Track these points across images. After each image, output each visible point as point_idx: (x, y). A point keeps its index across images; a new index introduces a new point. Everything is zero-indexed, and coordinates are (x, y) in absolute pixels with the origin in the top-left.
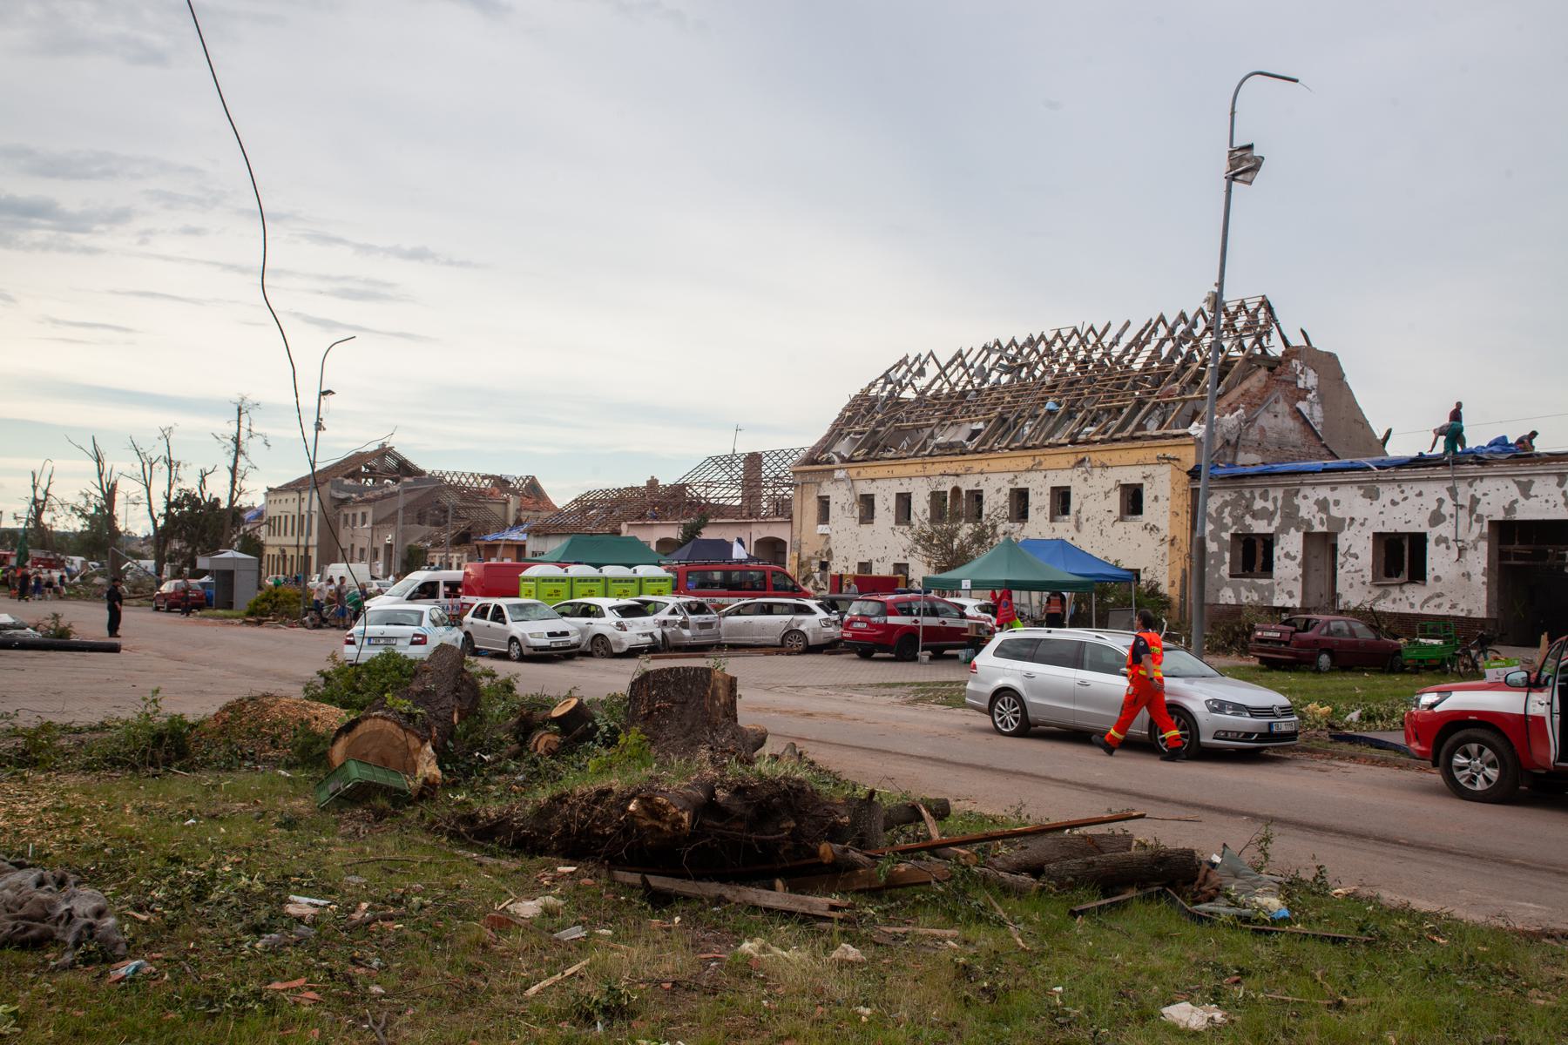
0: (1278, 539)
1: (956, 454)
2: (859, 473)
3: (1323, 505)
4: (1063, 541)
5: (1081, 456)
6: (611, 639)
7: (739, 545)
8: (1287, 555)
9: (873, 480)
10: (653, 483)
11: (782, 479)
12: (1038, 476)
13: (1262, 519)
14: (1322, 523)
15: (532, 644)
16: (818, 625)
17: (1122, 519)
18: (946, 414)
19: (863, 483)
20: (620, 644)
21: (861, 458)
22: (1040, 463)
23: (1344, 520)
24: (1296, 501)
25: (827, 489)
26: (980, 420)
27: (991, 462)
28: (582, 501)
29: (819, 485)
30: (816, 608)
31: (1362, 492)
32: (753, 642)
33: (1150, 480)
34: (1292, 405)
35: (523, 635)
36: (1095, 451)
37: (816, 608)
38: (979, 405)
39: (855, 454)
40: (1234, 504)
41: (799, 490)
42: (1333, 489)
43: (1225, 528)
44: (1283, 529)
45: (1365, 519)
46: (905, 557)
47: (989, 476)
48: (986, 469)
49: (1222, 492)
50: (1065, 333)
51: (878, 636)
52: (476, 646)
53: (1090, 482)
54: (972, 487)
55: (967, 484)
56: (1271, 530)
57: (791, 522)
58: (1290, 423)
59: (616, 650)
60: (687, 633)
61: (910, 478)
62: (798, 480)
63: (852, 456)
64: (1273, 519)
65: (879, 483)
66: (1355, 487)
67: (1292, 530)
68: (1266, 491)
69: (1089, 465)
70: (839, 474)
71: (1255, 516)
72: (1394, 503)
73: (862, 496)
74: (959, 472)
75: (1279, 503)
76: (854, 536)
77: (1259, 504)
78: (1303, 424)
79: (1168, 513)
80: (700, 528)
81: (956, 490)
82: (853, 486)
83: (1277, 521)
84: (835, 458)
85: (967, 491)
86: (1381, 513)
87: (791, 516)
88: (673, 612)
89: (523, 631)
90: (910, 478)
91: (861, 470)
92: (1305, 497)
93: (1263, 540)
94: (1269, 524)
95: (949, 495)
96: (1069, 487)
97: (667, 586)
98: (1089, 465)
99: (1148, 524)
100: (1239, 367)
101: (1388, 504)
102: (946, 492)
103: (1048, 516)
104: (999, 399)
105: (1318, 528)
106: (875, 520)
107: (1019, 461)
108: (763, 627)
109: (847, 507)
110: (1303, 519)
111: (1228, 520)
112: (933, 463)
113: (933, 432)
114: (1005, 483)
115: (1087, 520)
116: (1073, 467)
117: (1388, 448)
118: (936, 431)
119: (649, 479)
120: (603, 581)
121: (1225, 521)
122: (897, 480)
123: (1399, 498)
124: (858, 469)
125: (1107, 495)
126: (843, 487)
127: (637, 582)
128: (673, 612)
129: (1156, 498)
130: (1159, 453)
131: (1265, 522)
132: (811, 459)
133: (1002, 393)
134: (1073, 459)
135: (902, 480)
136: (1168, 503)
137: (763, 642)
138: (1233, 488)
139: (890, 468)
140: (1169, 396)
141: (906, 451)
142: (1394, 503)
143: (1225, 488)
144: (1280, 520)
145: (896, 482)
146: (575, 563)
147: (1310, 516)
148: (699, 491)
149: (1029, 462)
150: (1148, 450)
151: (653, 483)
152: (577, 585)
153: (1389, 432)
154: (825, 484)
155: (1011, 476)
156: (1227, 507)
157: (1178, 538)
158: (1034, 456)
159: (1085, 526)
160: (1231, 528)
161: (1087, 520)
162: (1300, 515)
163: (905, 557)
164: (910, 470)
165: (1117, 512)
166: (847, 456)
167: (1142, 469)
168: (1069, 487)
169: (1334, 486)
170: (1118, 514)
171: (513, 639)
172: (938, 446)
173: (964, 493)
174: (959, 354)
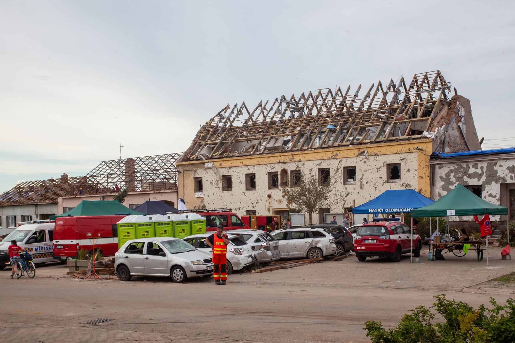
0: (485, 188)
1: (280, 152)
2: (221, 164)
4: (387, 191)
5: (362, 151)
6: (232, 261)
7: (182, 203)
8: (490, 195)
9: (230, 167)
10: (65, 177)
11: (158, 170)
12: (336, 162)
13: (474, 178)
15: (195, 269)
16: (329, 243)
17: (388, 182)
18: (265, 133)
19: (224, 169)
20: (238, 264)
21: (218, 157)
22: (337, 155)
24: (495, 168)
25: (200, 173)
26: (288, 135)
27: (305, 155)
28: (20, 188)
29: (195, 171)
30: (325, 233)
32: (289, 257)
33: (405, 161)
34: (457, 124)
35: (186, 263)
36: (370, 148)
37: (325, 233)
38: (285, 128)
39: (214, 155)
40: (456, 171)
41: (182, 174)
43: (452, 183)
44: (488, 182)
46: (253, 207)
48: (303, 159)
49: (449, 165)
50: (324, 92)
51: (386, 247)
52: (131, 274)
53: (368, 163)
54: (293, 169)
55: (291, 167)
56: (480, 183)
57: (177, 192)
58: (456, 133)
59: (235, 268)
60: (269, 253)
61: (254, 166)
62: (180, 169)
63: (212, 156)
64: (481, 178)
65: (234, 169)
67: (493, 183)
68: (477, 164)
69: (367, 155)
70: (206, 165)
71: (470, 176)
73: (223, 176)
74: (285, 161)
75: (485, 169)
76: (219, 197)
77: (472, 170)
78: (460, 133)
79: (416, 177)
80: (124, 197)
81: (284, 171)
82: (218, 171)
83: (484, 179)
84: (202, 157)
85: (291, 171)
87: (177, 189)
88: (258, 240)
89: (185, 260)
90: (254, 166)
91: (222, 163)
92: (501, 166)
93: (473, 188)
94: (479, 180)
95: (279, 173)
96: (355, 167)
97: (203, 226)
98: (367, 155)
99: (404, 183)
100: (438, 104)
102: (277, 172)
104: (296, 124)
106: (232, 189)
107: (323, 154)
108: (295, 247)
109: (214, 182)
110: (500, 177)
111: (453, 179)
112: (269, 157)
113: (260, 142)
114: (315, 166)
115: (367, 183)
116: (357, 156)
117: (482, 146)
118: (262, 141)
119: (63, 174)
120: (171, 224)
121: (451, 180)
122: (246, 167)
124: (220, 162)
125: (378, 169)
126: (211, 172)
127: (189, 223)
128: (258, 240)
129: (409, 170)
130: (416, 146)
131: (476, 179)
132: (187, 158)
133: (297, 121)
134: (357, 152)
135: (249, 167)
136: (416, 172)
137: (295, 256)
138: (456, 163)
139: (241, 161)
140: (403, 120)
141: (245, 152)
143: (450, 163)
144: (485, 178)
145: (246, 168)
146: (127, 215)
147: (504, 175)
148: (98, 179)
149: (330, 155)
151: (65, 177)
152: (158, 227)
153: (483, 139)
154: (199, 171)
155: (318, 162)
157: (423, 190)
158: (333, 151)
159: (366, 186)
160: (455, 183)
161: (367, 183)
162: (498, 175)
163: (253, 207)
164: (254, 161)
165: (385, 178)
166: (210, 156)
167: (400, 155)
168: (355, 167)
170: (386, 179)
171: (175, 267)
172: (266, 148)
173: (289, 172)
174: (260, 105)
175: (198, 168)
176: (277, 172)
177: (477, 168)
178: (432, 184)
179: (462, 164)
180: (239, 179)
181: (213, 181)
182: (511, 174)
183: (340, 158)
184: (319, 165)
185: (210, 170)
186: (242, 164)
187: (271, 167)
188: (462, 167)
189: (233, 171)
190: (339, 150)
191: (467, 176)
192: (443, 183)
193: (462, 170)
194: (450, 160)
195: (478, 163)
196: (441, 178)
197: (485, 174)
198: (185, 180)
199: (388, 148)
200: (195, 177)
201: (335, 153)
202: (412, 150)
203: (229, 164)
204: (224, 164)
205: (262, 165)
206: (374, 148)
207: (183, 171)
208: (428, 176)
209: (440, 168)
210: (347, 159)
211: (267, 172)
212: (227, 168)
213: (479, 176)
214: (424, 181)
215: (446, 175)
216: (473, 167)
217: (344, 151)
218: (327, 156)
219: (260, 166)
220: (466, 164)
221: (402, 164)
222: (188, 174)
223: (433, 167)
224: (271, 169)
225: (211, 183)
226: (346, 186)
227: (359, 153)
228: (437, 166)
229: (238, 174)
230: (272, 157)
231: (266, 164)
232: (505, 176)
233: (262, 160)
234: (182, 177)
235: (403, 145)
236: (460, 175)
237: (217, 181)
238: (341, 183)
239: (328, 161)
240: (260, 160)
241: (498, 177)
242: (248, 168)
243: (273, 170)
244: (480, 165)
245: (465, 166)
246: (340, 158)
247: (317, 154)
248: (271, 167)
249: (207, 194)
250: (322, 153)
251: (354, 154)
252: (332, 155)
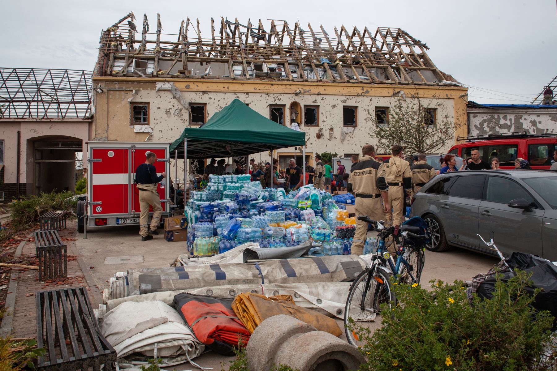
2: (188, 87)
3: (534, 123)
5: (397, 90)
9: (204, 92)
12: (366, 100)
13: (505, 129)
14: (534, 131)
19: (194, 94)
22: (367, 92)
24: (521, 121)
25: (144, 96)
27: (326, 88)
29: (137, 93)
31: (551, 118)
33: (442, 106)
36: (407, 88)
40: (489, 121)
41: (105, 96)
42: (538, 116)
47: (324, 96)
49: (482, 115)
55: (305, 101)
61: (247, 94)
64: (511, 129)
65: (211, 95)
66: (548, 116)
68: (506, 116)
70: (159, 85)
71: (502, 127)
75: (513, 122)
77: (502, 122)
90: (247, 94)
91: (191, 84)
92: (525, 119)
94: (509, 131)
102: (284, 106)
109: (172, 111)
112: (272, 85)
114: (339, 102)
121: (485, 129)
124: (188, 83)
134: (391, 92)
139: (226, 86)
149: (359, 91)
150: (441, 91)
155: (344, 98)
158: (363, 87)
162: (523, 127)
169: (538, 115)
175: (141, 89)
176: (284, 106)
177: (507, 120)
178: (469, 132)
179: (494, 115)
181: (171, 109)
182: (533, 127)
183: (371, 96)
184: (345, 101)
185: (166, 93)
186: (226, 90)
187: (274, 98)
188: (494, 118)
189: (210, 98)
190: (371, 87)
191: (499, 127)
192: (478, 132)
193: (494, 120)
194: (486, 110)
195: (507, 115)
196: (476, 126)
197: (513, 125)
198: (110, 105)
199: (426, 91)
200: (134, 101)
201: (365, 89)
202: (449, 96)
203: (203, 87)
204: (193, 87)
205: (260, 94)
206: (412, 90)
207: (108, 90)
208: (466, 124)
209: (474, 117)
210: (379, 97)
211: (268, 104)
212: (198, 93)
213: (509, 127)
214: (462, 129)
215: (480, 124)
216: (503, 118)
217: (376, 89)
218: (355, 91)
219: (257, 94)
220: (497, 115)
221: (439, 110)
222: (117, 96)
223: (468, 114)
224: (275, 100)
225: (168, 112)
227: (395, 93)
228: (471, 115)
229: (219, 103)
230: (278, 84)
231: (267, 94)
233: (261, 87)
234: (105, 100)
235: (441, 90)
236: (492, 125)
237: (179, 111)
239: (356, 98)
240: (257, 87)
242: (236, 96)
243: (278, 103)
244: (509, 117)
245: (496, 117)
246: (371, 96)
247: (342, 88)
248: (274, 98)
249: (157, 128)
250: (349, 88)
251: (389, 93)
252: (362, 91)
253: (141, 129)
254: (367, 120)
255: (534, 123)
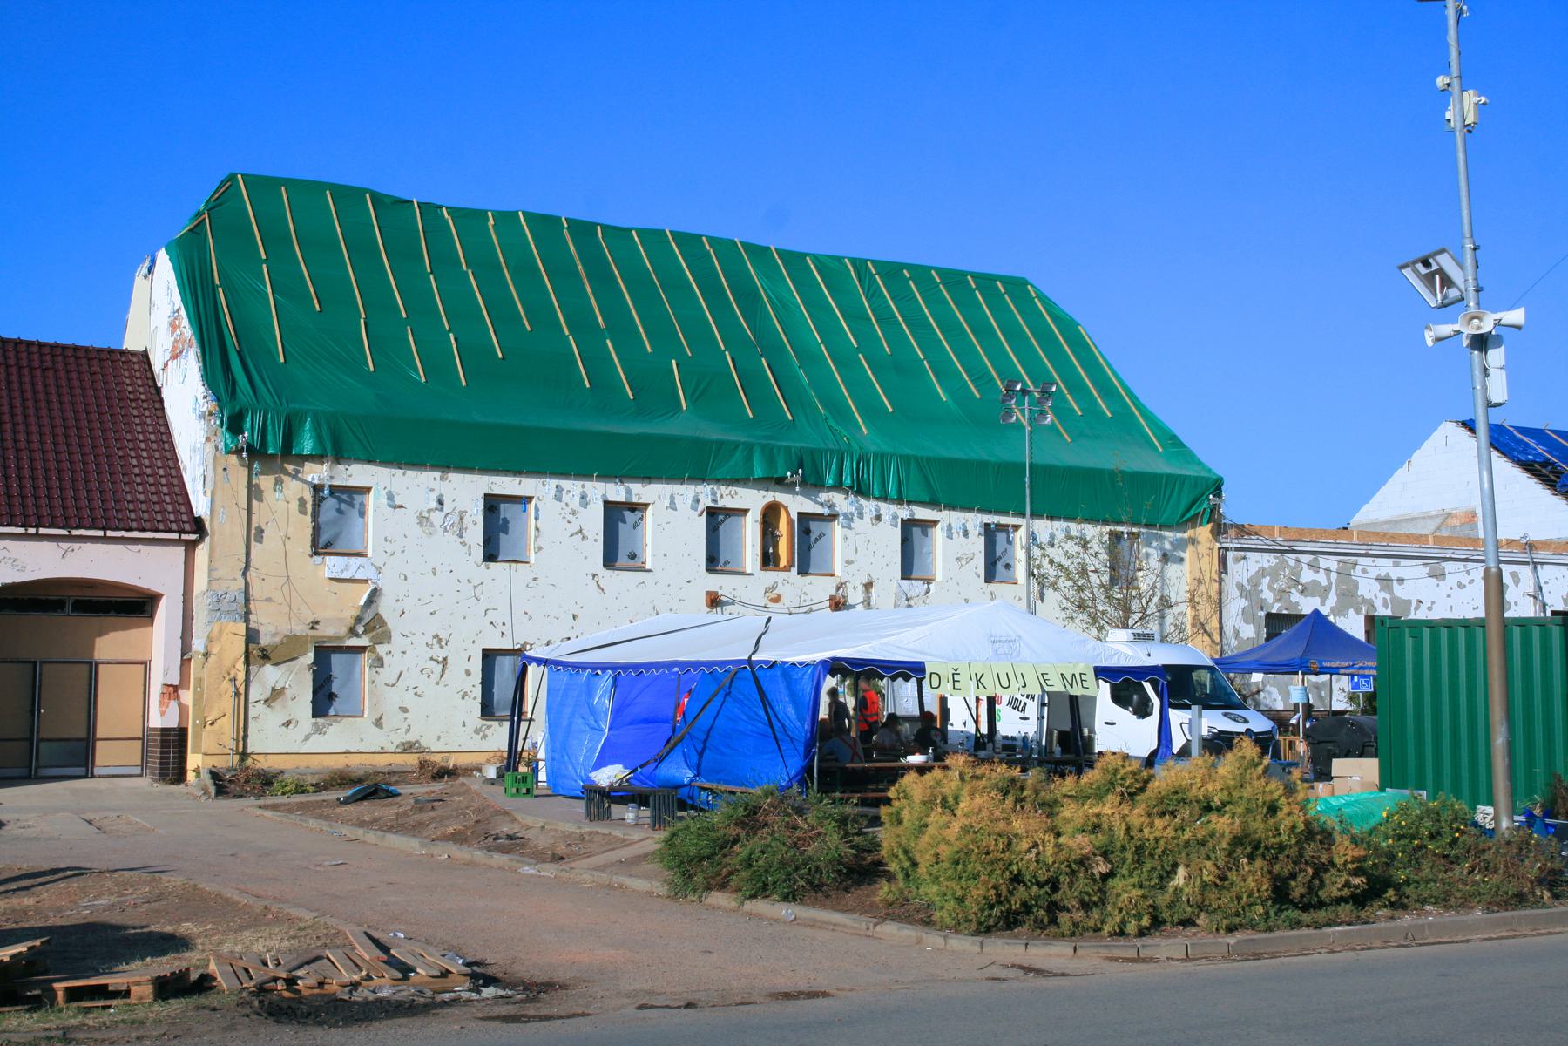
3: (1385, 582)
14: (1385, 605)
23: (1409, 602)
40: (1274, 573)
42: (1396, 565)
45: (1433, 603)
67: (1351, 611)
72: (1461, 586)
77: (1307, 576)
86: (1449, 596)
101: (1455, 586)
103: (982, 571)
105: (1382, 611)
110: (1364, 601)
123: (1465, 581)
142: (1461, 586)
156: (1264, 576)
162: (1359, 593)
180: (571, 518)
191: (1298, 590)
192: (1244, 603)
197: (1334, 586)
209: (1237, 560)
213: (1323, 593)
225: (423, 520)
226: (992, 586)
228: (1230, 555)
232: (1374, 598)
236: (1281, 584)
238: (979, 576)
241: (1360, 599)
253: (347, 568)
254: (964, 562)
255: (1385, 582)
